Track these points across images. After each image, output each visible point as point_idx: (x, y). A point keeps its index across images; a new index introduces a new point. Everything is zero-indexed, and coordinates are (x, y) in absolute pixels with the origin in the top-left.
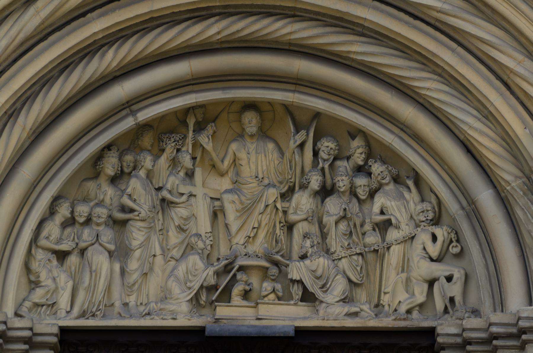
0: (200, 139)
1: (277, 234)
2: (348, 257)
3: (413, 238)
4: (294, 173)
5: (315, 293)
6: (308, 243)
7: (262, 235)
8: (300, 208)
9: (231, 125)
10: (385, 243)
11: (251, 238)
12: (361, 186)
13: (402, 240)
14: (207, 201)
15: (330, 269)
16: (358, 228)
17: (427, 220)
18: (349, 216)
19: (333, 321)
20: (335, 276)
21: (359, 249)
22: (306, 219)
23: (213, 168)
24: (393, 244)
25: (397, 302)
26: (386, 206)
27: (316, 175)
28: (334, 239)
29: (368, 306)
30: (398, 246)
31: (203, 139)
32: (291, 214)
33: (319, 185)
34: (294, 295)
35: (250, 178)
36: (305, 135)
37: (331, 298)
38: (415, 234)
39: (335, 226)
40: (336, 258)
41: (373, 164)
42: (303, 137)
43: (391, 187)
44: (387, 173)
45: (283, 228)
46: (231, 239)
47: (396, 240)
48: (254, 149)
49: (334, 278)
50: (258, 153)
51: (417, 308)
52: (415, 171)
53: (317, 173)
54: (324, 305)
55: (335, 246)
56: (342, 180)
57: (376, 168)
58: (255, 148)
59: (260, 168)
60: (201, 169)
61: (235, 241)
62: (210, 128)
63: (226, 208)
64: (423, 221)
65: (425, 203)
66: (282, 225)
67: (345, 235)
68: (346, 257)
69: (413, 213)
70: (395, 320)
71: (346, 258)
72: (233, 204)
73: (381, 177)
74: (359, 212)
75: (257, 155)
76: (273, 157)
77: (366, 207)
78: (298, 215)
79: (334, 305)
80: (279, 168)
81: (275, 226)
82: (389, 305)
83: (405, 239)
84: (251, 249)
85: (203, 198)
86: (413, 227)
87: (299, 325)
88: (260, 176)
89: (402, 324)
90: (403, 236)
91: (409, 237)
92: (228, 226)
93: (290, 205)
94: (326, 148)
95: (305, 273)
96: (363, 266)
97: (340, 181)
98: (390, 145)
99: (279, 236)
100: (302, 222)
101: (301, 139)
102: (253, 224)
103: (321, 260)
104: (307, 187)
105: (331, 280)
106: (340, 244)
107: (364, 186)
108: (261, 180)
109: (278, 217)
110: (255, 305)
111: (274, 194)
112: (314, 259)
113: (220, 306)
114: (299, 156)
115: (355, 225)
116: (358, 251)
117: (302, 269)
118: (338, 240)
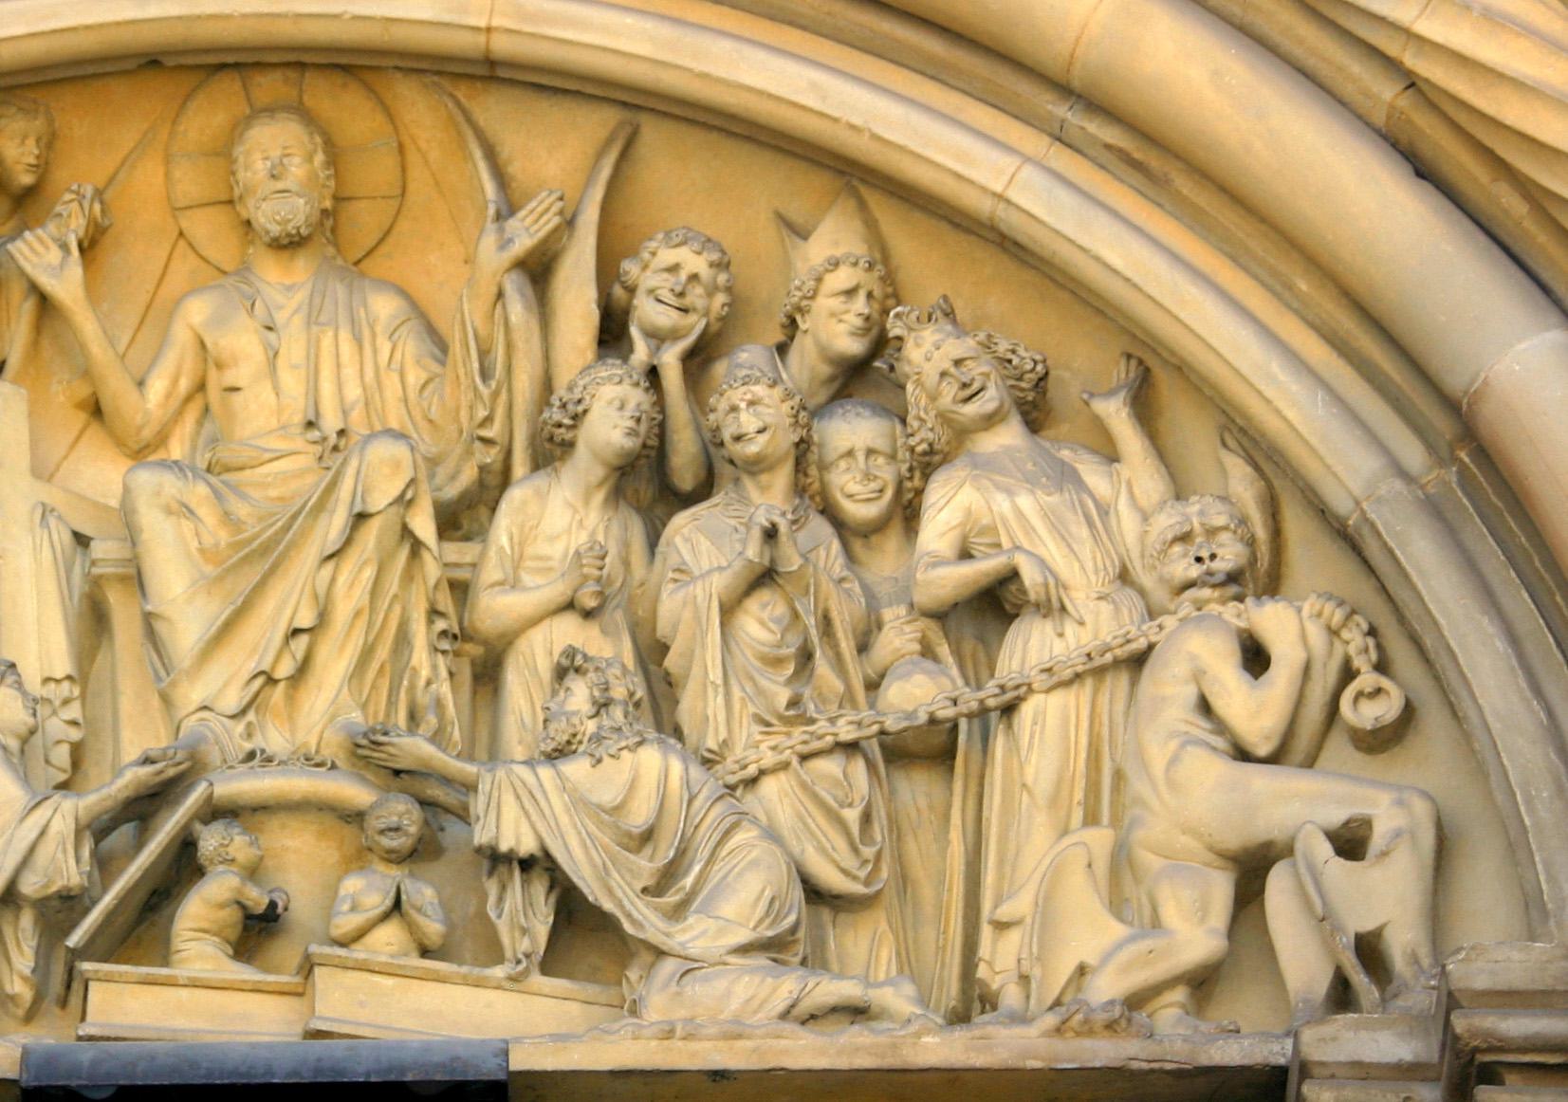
0: (22, 254)
1: (415, 671)
2: (795, 761)
3: (1138, 661)
4: (503, 396)
5: (619, 914)
6: (579, 695)
7: (334, 664)
8: (540, 558)
9: (185, 224)
10: (991, 683)
11: (282, 686)
12: (850, 453)
13: (1080, 669)
14: (55, 537)
15: (697, 804)
16: (840, 635)
17: (1210, 573)
18: (795, 568)
19: (721, 1044)
20: (727, 834)
21: (851, 723)
22: (570, 606)
23: (95, 427)
24: (1029, 685)
25: (1065, 970)
26: (985, 521)
27: (617, 379)
28: (719, 681)
29: (909, 989)
30: (1057, 699)
31: (32, 249)
32: (492, 585)
33: (631, 423)
34: (506, 939)
35: (282, 432)
36: (555, 209)
37: (704, 933)
38: (1151, 647)
39: (722, 624)
40: (732, 779)
41: (910, 329)
42: (545, 218)
43: (1010, 436)
44: (985, 369)
45: (445, 645)
46: (173, 684)
47: (1049, 670)
48: (296, 311)
49: (720, 844)
50: (317, 324)
51: (1179, 994)
52: (1133, 363)
53: (620, 372)
54: (669, 966)
55: (722, 717)
56: (751, 403)
57: (927, 346)
58: (305, 308)
59: (327, 388)
60: (23, 391)
61: (191, 694)
62: (75, 205)
63: (145, 536)
64: (1190, 585)
65: (1194, 499)
66: (441, 625)
67: (777, 662)
68: (785, 766)
69: (1135, 554)
70: (1058, 1030)
71: (782, 776)
72: (184, 521)
73: (956, 386)
74: (845, 573)
75: (315, 329)
76: (398, 356)
77: (884, 561)
78: (525, 589)
79: (725, 964)
80: (425, 404)
81: (403, 639)
82: (1024, 979)
83: (1098, 662)
84: (275, 739)
85: (32, 521)
86: (1136, 617)
87: (537, 1067)
88: (331, 423)
89: (1103, 1052)
90: (1086, 650)
91: (1118, 652)
92: (160, 627)
93: (483, 554)
94: (665, 275)
95: (564, 820)
96: (874, 814)
97: (743, 405)
98: (1001, 211)
99: (429, 683)
100: (547, 623)
101: (537, 231)
102: (288, 613)
103: (650, 759)
104: (569, 446)
105: (703, 854)
106: (752, 709)
107: (870, 452)
108: (333, 439)
109: (422, 589)
110: (298, 979)
111: (397, 465)
112: (612, 751)
113: (108, 979)
114: (527, 308)
115: (826, 623)
116: (847, 733)
117: (547, 799)
118: (737, 693)
